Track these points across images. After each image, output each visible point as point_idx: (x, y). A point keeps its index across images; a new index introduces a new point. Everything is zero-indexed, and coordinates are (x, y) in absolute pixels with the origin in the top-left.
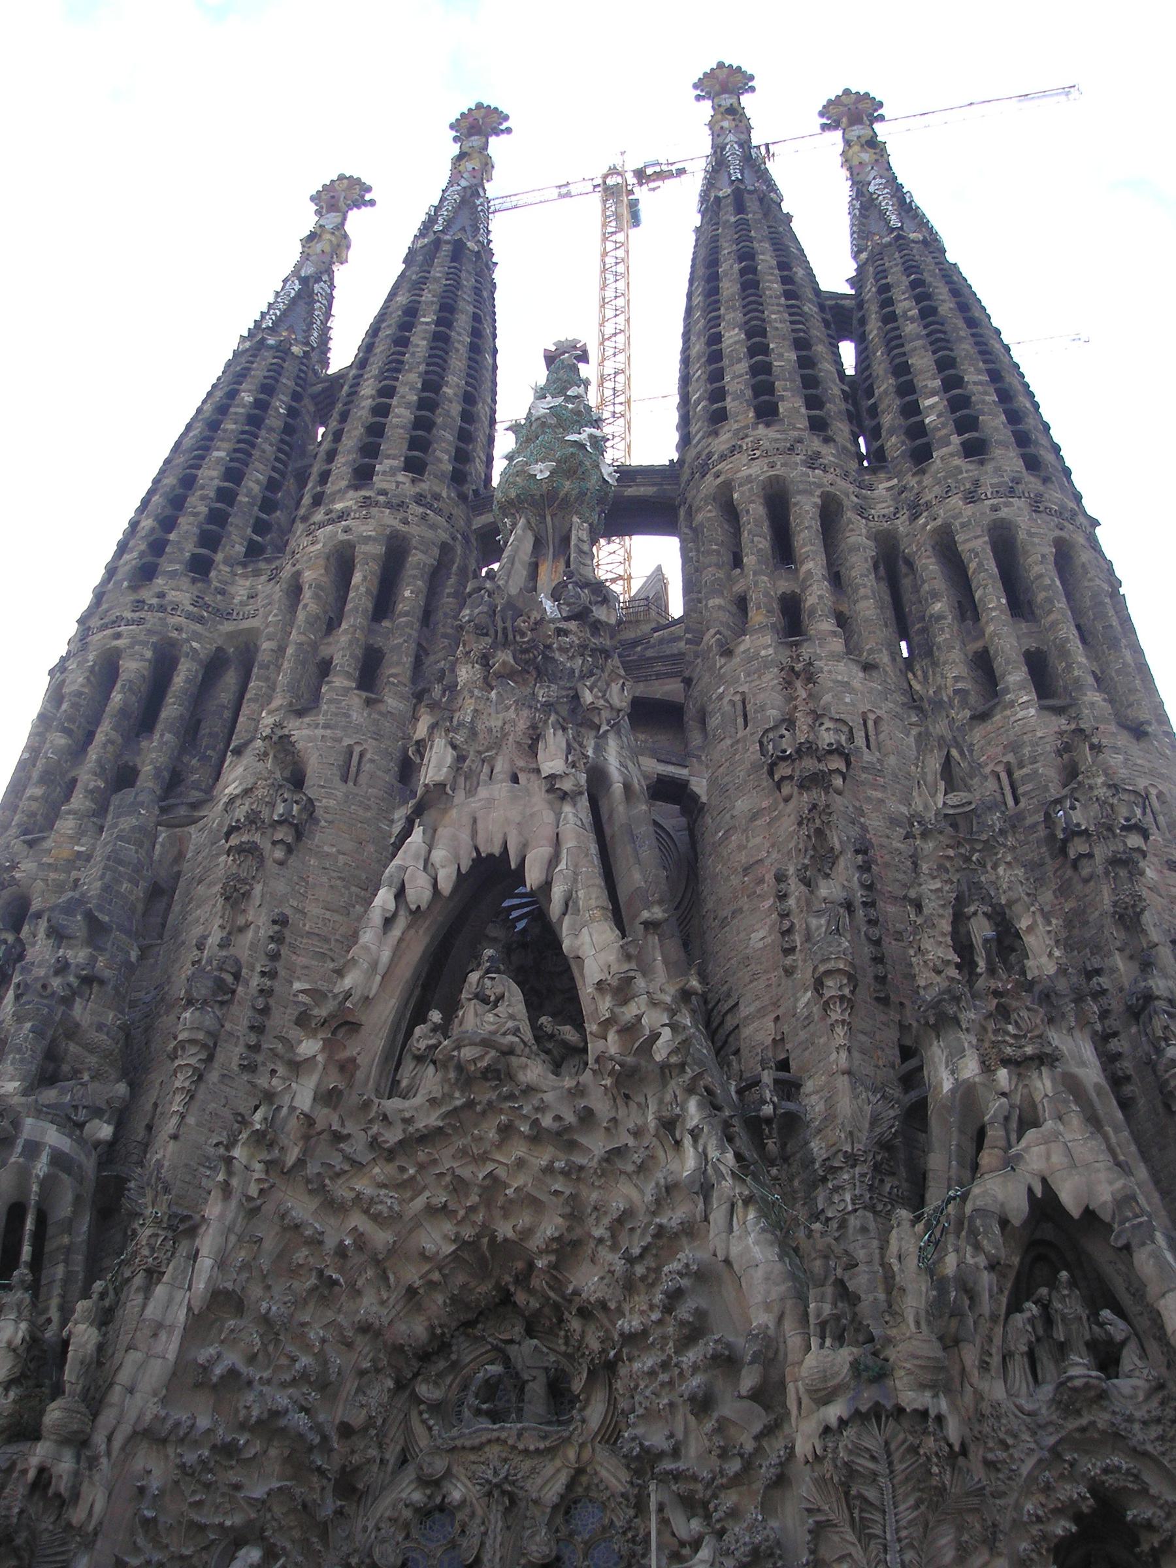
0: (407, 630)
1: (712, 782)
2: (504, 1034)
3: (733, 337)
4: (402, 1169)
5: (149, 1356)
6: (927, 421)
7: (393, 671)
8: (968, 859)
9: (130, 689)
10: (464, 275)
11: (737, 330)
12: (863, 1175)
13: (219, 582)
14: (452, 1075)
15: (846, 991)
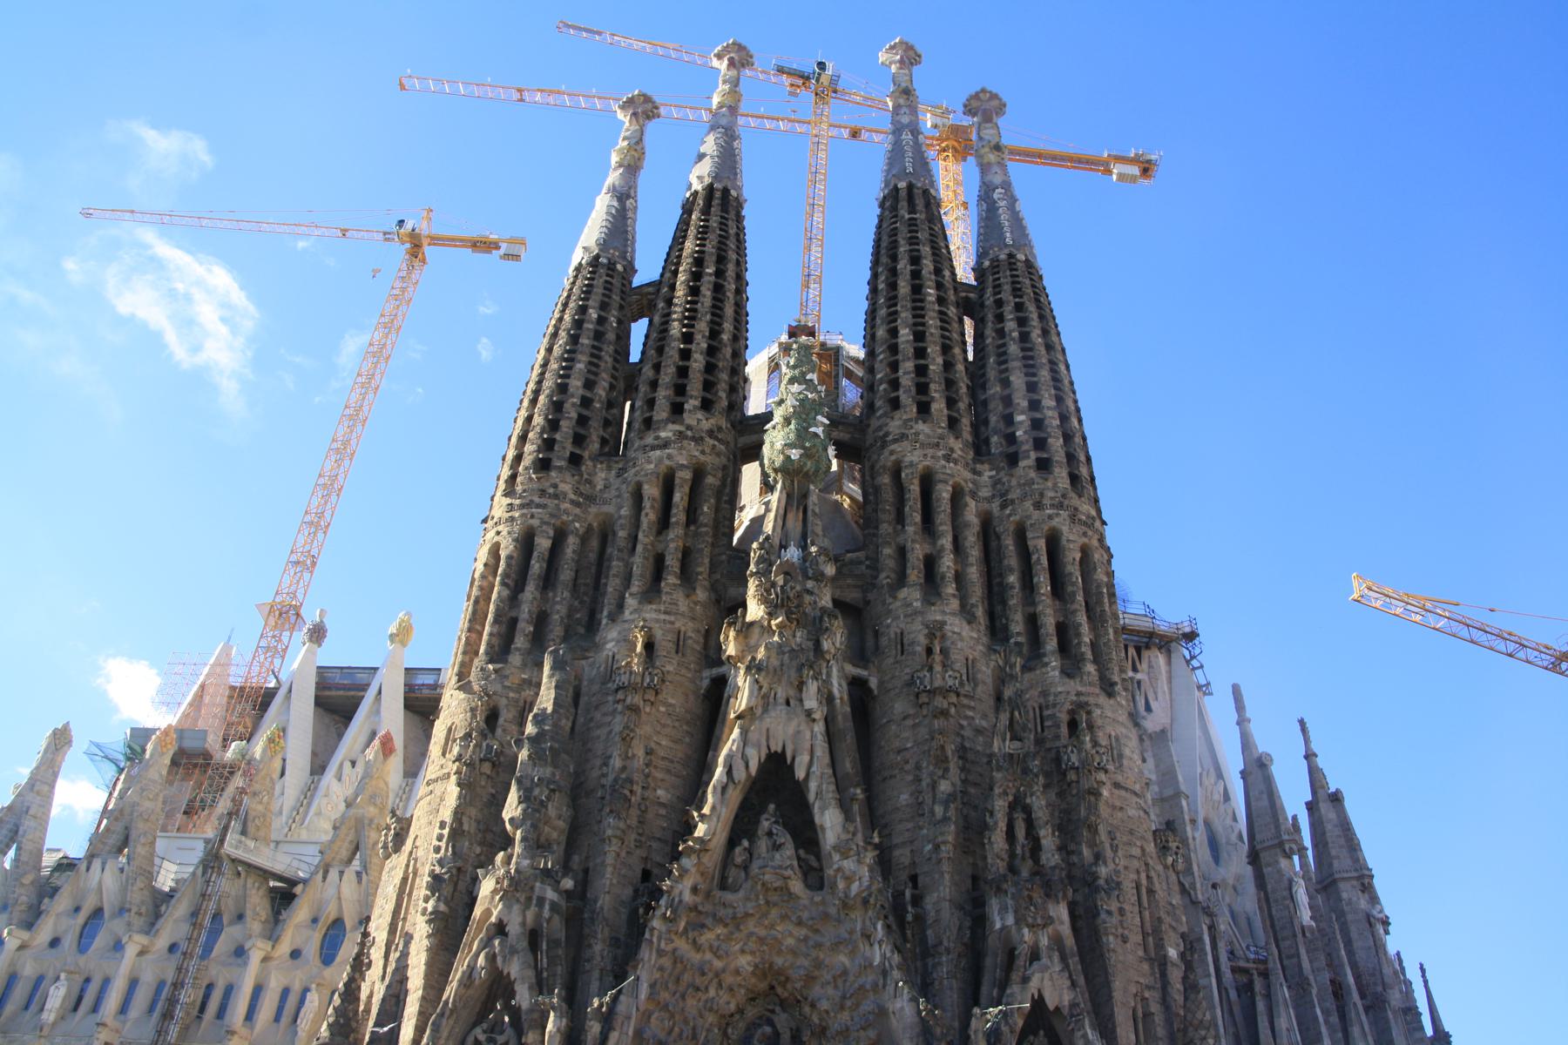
0: (707, 538)
1: (881, 683)
2: (786, 868)
3: (905, 334)
4: (732, 933)
5: (621, 1033)
6: (1018, 434)
7: (700, 569)
8: (1018, 790)
9: (543, 559)
10: (730, 223)
11: (907, 330)
12: (952, 960)
13: (588, 474)
14: (759, 887)
15: (951, 855)
